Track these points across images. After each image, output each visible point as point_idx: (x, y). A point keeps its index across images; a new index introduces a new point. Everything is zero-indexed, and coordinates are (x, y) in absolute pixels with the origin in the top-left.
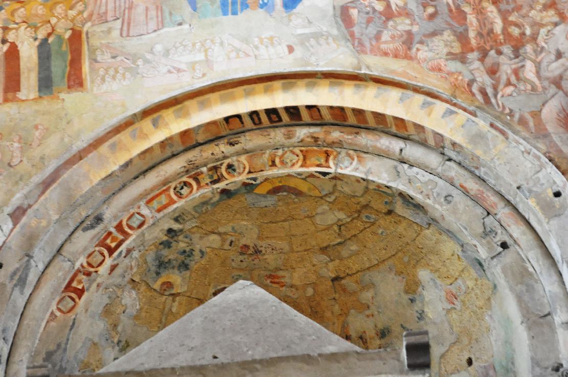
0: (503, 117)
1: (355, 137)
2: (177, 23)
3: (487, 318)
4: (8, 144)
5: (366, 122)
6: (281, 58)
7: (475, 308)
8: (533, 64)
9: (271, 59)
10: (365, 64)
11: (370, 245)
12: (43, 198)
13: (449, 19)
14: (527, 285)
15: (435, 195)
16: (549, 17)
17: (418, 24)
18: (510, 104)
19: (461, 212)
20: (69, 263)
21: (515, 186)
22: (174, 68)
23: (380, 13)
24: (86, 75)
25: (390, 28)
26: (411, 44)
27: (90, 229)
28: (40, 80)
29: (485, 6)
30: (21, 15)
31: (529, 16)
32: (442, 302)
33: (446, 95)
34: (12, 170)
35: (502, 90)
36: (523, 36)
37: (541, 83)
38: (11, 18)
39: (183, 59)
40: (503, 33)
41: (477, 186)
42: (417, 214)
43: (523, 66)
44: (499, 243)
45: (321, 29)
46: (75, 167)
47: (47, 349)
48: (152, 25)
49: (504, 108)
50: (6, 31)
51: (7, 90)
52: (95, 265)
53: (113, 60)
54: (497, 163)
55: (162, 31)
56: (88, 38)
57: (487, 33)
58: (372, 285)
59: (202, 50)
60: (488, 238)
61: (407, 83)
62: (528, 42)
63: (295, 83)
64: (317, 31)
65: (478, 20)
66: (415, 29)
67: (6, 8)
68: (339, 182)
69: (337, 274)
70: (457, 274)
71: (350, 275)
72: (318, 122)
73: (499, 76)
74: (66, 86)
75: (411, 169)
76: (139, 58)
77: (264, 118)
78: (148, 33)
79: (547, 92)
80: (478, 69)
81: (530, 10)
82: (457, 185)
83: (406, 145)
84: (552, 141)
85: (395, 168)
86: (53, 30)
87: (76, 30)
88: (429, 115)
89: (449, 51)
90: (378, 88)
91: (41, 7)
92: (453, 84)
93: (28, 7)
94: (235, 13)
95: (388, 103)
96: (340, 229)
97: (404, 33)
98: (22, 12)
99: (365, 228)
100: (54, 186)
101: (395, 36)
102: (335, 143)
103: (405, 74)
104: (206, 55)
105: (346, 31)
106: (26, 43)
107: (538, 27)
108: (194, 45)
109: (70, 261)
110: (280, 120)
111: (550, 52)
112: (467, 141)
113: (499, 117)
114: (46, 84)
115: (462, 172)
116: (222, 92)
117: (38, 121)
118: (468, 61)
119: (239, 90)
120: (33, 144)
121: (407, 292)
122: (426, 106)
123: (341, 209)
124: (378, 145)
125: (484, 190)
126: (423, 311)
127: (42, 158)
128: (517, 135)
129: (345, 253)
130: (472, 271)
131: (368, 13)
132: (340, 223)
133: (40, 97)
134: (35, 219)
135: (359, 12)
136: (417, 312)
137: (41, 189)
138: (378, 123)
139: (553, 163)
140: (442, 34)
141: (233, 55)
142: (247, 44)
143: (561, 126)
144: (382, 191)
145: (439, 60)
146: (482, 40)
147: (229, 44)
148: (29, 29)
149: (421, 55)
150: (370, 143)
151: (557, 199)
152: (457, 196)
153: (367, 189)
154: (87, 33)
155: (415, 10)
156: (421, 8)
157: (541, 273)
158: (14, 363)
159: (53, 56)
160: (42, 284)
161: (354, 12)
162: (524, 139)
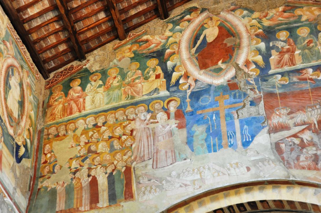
2: (183, 159)
5: (295, 208)
6: (243, 174)
9: (237, 175)
22: (183, 184)
23: (298, 145)
25: (304, 153)
26: (318, 161)
28: (109, 196)
30: (98, 160)
38: (92, 162)
39: (188, 179)
48: (170, 161)
51: (91, 203)
53: (149, 182)
55: (175, 164)
56: (134, 171)
59: (198, 173)
61: (318, 184)
63: (253, 188)
64: (262, 157)
67: (90, 157)
72: (268, 210)
74: (124, 198)
76: (163, 180)
77: (236, 209)
78: (168, 166)
86: (115, 167)
87: (128, 167)
90: (301, 188)
91: (108, 155)
93: (101, 156)
94: (215, 151)
97: (313, 156)
101: (307, 157)
104: (201, 176)
105: (279, 156)
106: (101, 176)
108: (193, 170)
110: (246, 210)
114: (113, 198)
116: (211, 196)
119: (221, 194)
131: (291, 145)
135: (285, 145)
138: (302, 208)
141: (216, 174)
142: (224, 167)
147: (213, 169)
148: (102, 168)
154: (134, 168)
159: (116, 182)
161: (283, 146)
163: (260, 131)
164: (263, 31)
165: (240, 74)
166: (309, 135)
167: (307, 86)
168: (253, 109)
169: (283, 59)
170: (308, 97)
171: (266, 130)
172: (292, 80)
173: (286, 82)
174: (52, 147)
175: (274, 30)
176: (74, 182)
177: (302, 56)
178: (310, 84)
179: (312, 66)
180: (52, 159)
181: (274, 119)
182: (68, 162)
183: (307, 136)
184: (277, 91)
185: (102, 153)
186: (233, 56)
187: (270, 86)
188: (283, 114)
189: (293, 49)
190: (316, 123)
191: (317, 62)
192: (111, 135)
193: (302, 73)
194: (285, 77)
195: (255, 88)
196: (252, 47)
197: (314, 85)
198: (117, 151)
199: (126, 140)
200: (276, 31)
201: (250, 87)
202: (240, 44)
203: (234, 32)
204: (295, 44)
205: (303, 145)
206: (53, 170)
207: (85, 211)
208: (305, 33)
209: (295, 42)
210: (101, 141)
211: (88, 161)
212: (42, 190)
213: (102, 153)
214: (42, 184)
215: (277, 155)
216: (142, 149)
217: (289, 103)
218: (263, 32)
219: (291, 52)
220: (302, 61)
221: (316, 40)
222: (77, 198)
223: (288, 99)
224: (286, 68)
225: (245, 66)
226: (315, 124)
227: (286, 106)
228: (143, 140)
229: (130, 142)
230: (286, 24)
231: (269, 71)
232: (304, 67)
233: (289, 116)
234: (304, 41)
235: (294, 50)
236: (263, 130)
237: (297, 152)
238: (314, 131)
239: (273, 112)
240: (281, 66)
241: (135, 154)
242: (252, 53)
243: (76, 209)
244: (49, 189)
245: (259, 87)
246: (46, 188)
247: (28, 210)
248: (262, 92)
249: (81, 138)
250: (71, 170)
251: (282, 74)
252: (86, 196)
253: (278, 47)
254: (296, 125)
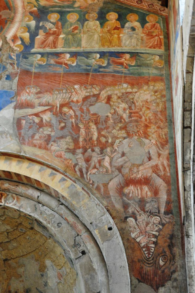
0: (88, 185)
1: (16, 187)
3: (74, 290)
5: (23, 181)
7: (70, 284)
8: (109, 158)
10: (24, 151)
11: (23, 244)
13: (71, 130)
14: (91, 275)
15: (53, 222)
16: (122, 134)
17: (55, 131)
18: (94, 178)
19: (64, 232)
21: (90, 222)
23: (37, 124)
26: (49, 142)
29: (91, 125)
31: (111, 132)
32: (56, 278)
33: (62, 170)
35: (90, 171)
36: (107, 143)
37: (111, 169)
40: (97, 141)
41: (73, 220)
42: (45, 231)
43: (104, 159)
44: (81, 251)
45: (5, 129)
49: (90, 180)
54: (83, 209)
57: (89, 140)
58: (24, 265)
60: (76, 248)
62: (109, 146)
65: (86, 132)
66: (53, 134)
68: (6, 210)
69: (6, 258)
70: (63, 264)
71: (13, 259)
73: (91, 163)
75: (43, 207)
79: (113, 173)
80: (80, 158)
81: (113, 129)
82: (64, 217)
83: (41, 194)
84: (111, 200)
85: (35, 205)
88: (53, 180)
89: (67, 147)
92: (66, 165)
95: (33, 172)
96: (8, 234)
97: (47, 136)
99: (21, 235)
101: (41, 137)
102: (7, 190)
103: (42, 158)
107: (115, 139)
111: (119, 153)
112: (69, 196)
113: (86, 185)
115: (67, 211)
118: (77, 153)
121: (40, 270)
122: (51, 175)
123: (8, 224)
124: (27, 193)
125: (76, 223)
126: (47, 282)
128: (93, 195)
129: (10, 247)
130: (69, 264)
131: (30, 123)
132: (8, 231)
135: (26, 122)
136: (44, 282)
138: (28, 181)
139: (109, 212)
140: (66, 138)
143: (118, 193)
144: (27, 217)
145: (61, 152)
146: (86, 143)
149: (53, 148)
150: (23, 191)
151: (109, 231)
152: (64, 224)
153: (20, 216)
155: (55, 123)
156: (58, 123)
157: (98, 270)
161: (24, 122)
162: (97, 198)
163: (8, 105)
164: (38, 9)
165: (6, 47)
166: (49, 116)
167: (60, 70)
168: (7, 83)
169: (48, 40)
170: (59, 80)
171: (13, 105)
172: (49, 62)
173: (44, 63)
175: (47, 11)
177: (65, 41)
178: (64, 69)
179: (71, 52)
181: (23, 96)
183: (47, 117)
184: (34, 70)
186: (4, 28)
187: (28, 64)
188: (32, 93)
189: (59, 32)
190: (58, 106)
191: (76, 49)
193: (60, 57)
194: (44, 57)
195: (14, 64)
196: (23, 23)
197: (67, 71)
200: (49, 12)
201: (11, 62)
202: (14, 18)
203: (12, 5)
204: (62, 28)
205: (41, 125)
208: (74, 19)
209: (63, 26)
215: (16, 130)
217: (40, 83)
218: (37, 11)
219: (56, 34)
220: (63, 45)
221: (81, 28)
223: (41, 79)
224: (48, 50)
225: (12, 40)
226: (57, 107)
227: (37, 85)
230: (60, 7)
231: (31, 49)
232: (63, 51)
233: (37, 96)
234: (71, 26)
235: (60, 33)
236: (11, 104)
237: (34, 130)
238: (54, 113)
239: (24, 89)
240: (44, 46)
242: (22, 29)
245: (19, 63)
248: (20, 68)
251: (42, 54)
253: (46, 28)
254: (40, 105)
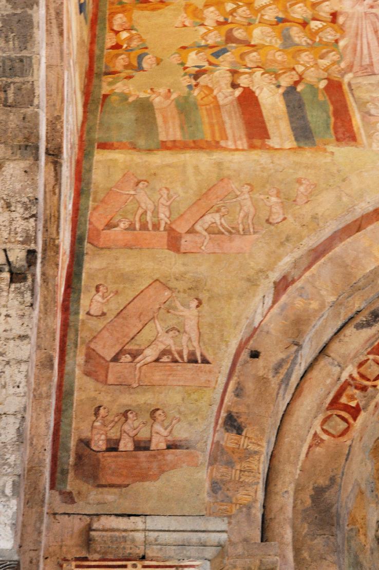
4: (262, 197)
12: (307, 274)
20: (338, 369)
24: (359, 129)
27: (365, 327)
28: (294, 129)
30: (254, 59)
34: (272, 227)
38: (241, 62)
46: (349, 240)
47: (315, 483)
50: (236, 75)
51: (250, 136)
52: (372, 379)
56: (351, 90)
67: (233, 50)
74: (334, 138)
86: (301, 78)
87: (333, 80)
93: (261, 51)
98: (254, 56)
100: (322, 260)
106: (265, 89)
109: (340, 366)
117: (300, 174)
120: (298, 200)
127: (315, 218)
133: (300, 147)
134: (300, 298)
137: (310, 258)
148: (266, 75)
154: (349, 84)
158: (277, 493)
160: (306, 392)
174: (130, 19)
176: (196, 92)
180: (134, 44)
182: (175, 53)
185: (264, 46)
192: (281, 15)
198: (302, 48)
199: (320, 30)
206: (140, 63)
207: (237, 150)
210: (257, 23)
211: (228, 58)
212: (113, 98)
213: (263, 47)
214: (113, 87)
216: (365, 51)
222: (212, 125)
228: (364, 35)
229: (331, 35)
241: (348, 58)
243: (213, 143)
244: (131, 99)
246: (124, 97)
247: (86, 129)
249: (205, 11)
250: (185, 68)
252: (234, 125)
